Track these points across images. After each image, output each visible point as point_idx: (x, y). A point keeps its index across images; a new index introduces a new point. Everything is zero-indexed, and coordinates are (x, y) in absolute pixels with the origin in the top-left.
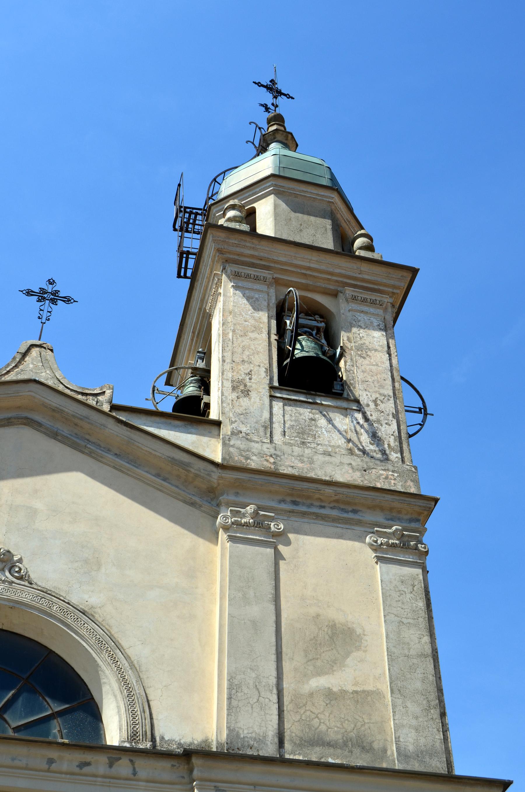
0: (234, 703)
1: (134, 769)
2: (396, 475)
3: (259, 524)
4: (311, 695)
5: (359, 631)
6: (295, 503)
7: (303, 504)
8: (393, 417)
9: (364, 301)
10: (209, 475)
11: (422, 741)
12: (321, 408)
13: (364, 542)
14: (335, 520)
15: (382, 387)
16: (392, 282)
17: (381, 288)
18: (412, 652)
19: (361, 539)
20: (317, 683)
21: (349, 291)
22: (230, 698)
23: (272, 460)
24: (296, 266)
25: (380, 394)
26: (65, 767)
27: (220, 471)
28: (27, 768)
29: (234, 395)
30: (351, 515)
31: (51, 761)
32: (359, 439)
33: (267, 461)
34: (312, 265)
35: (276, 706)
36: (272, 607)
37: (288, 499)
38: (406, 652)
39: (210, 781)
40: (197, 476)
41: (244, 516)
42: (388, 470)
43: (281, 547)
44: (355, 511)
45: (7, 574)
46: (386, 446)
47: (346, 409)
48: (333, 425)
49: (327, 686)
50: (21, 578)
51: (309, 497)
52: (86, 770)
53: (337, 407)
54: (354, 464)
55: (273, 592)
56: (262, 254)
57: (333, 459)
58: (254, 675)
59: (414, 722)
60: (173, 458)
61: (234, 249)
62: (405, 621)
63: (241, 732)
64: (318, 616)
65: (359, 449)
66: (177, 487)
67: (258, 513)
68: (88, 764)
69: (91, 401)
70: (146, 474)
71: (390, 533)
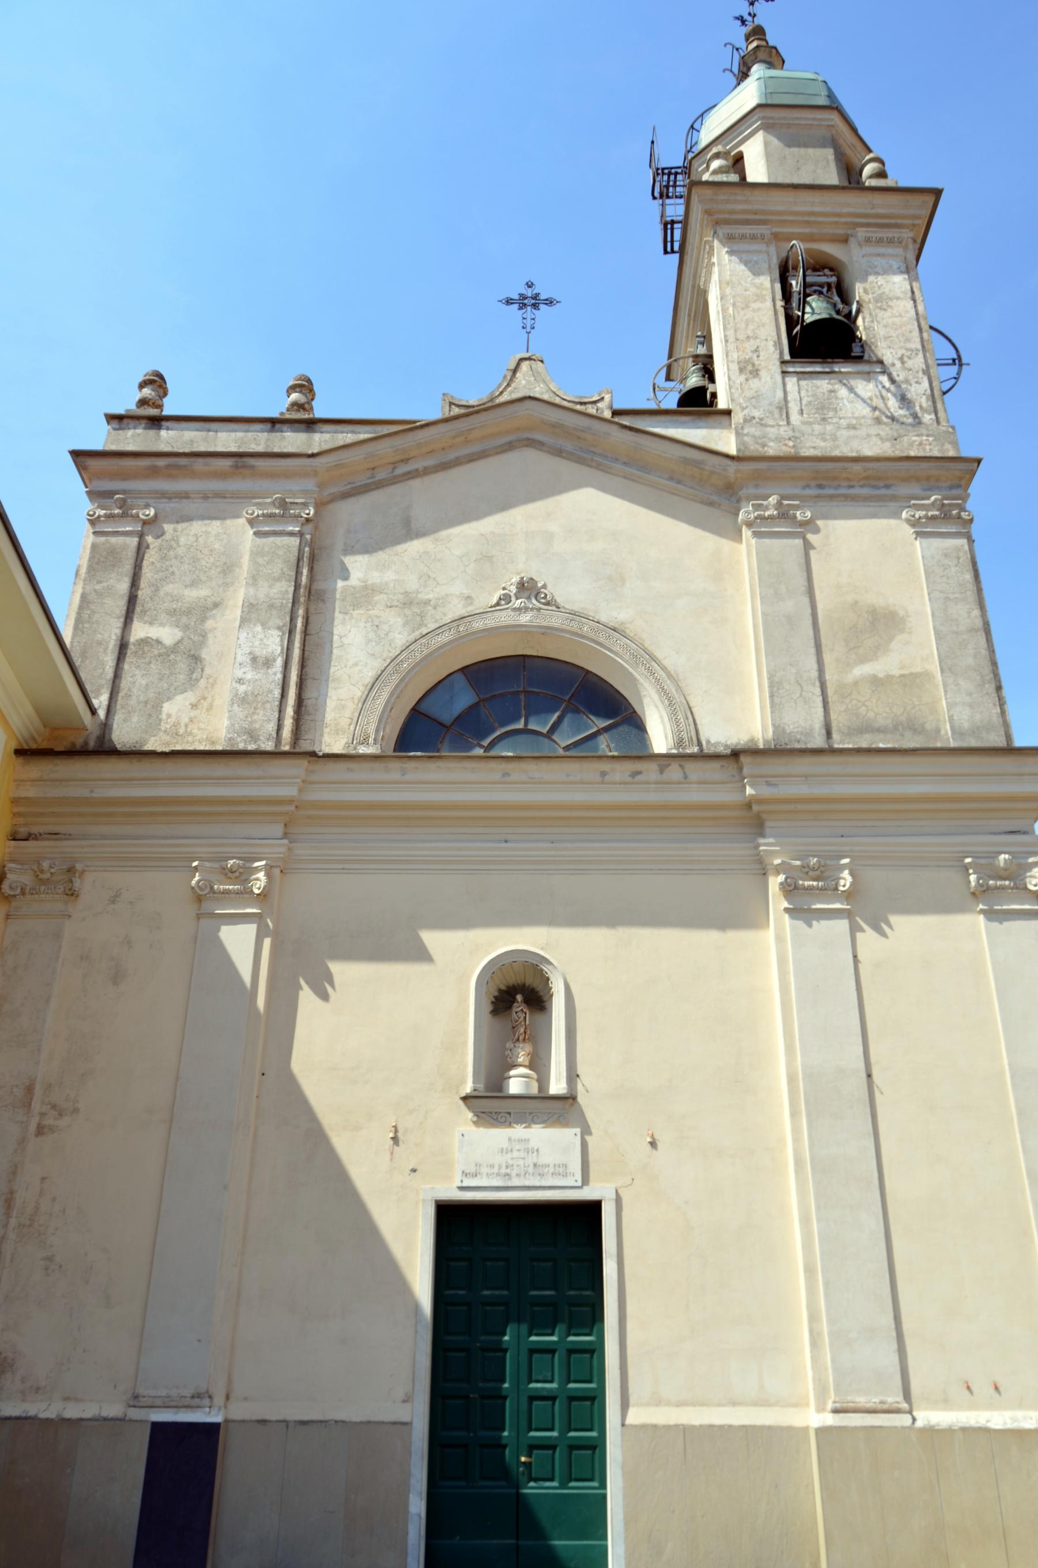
0: (777, 700)
1: (685, 773)
2: (931, 439)
3: (784, 515)
4: (856, 683)
5: (901, 613)
6: (820, 487)
7: (830, 487)
8: (924, 373)
9: (880, 241)
10: (725, 470)
11: (978, 717)
12: (840, 376)
13: (900, 518)
14: (866, 499)
15: (908, 340)
16: (911, 212)
17: (899, 221)
18: (962, 628)
19: (897, 515)
20: (860, 671)
21: (861, 233)
22: (772, 696)
23: (791, 444)
24: (797, 214)
25: (907, 350)
26: (618, 777)
27: (736, 463)
28: (582, 783)
29: (743, 378)
30: (883, 491)
31: (604, 774)
32: (886, 405)
33: (786, 445)
34: (817, 209)
35: (821, 698)
36: (806, 600)
37: (813, 483)
38: (955, 628)
39: (761, 776)
40: (712, 473)
41: (767, 508)
42: (922, 435)
43: (810, 537)
44: (887, 487)
45: (534, 601)
46: (917, 408)
47: (869, 373)
48: (856, 394)
49: (872, 672)
50: (548, 604)
51: (835, 478)
52: (638, 778)
53: (858, 373)
54: (882, 433)
55: (806, 584)
56: (756, 207)
57: (858, 433)
58: (794, 671)
59: (968, 699)
60: (685, 459)
61: (722, 207)
62: (951, 596)
63: (787, 727)
64: (856, 603)
65: (887, 417)
66: (692, 488)
67: (781, 504)
68: (639, 773)
69: (591, 410)
70: (657, 479)
71: (928, 505)
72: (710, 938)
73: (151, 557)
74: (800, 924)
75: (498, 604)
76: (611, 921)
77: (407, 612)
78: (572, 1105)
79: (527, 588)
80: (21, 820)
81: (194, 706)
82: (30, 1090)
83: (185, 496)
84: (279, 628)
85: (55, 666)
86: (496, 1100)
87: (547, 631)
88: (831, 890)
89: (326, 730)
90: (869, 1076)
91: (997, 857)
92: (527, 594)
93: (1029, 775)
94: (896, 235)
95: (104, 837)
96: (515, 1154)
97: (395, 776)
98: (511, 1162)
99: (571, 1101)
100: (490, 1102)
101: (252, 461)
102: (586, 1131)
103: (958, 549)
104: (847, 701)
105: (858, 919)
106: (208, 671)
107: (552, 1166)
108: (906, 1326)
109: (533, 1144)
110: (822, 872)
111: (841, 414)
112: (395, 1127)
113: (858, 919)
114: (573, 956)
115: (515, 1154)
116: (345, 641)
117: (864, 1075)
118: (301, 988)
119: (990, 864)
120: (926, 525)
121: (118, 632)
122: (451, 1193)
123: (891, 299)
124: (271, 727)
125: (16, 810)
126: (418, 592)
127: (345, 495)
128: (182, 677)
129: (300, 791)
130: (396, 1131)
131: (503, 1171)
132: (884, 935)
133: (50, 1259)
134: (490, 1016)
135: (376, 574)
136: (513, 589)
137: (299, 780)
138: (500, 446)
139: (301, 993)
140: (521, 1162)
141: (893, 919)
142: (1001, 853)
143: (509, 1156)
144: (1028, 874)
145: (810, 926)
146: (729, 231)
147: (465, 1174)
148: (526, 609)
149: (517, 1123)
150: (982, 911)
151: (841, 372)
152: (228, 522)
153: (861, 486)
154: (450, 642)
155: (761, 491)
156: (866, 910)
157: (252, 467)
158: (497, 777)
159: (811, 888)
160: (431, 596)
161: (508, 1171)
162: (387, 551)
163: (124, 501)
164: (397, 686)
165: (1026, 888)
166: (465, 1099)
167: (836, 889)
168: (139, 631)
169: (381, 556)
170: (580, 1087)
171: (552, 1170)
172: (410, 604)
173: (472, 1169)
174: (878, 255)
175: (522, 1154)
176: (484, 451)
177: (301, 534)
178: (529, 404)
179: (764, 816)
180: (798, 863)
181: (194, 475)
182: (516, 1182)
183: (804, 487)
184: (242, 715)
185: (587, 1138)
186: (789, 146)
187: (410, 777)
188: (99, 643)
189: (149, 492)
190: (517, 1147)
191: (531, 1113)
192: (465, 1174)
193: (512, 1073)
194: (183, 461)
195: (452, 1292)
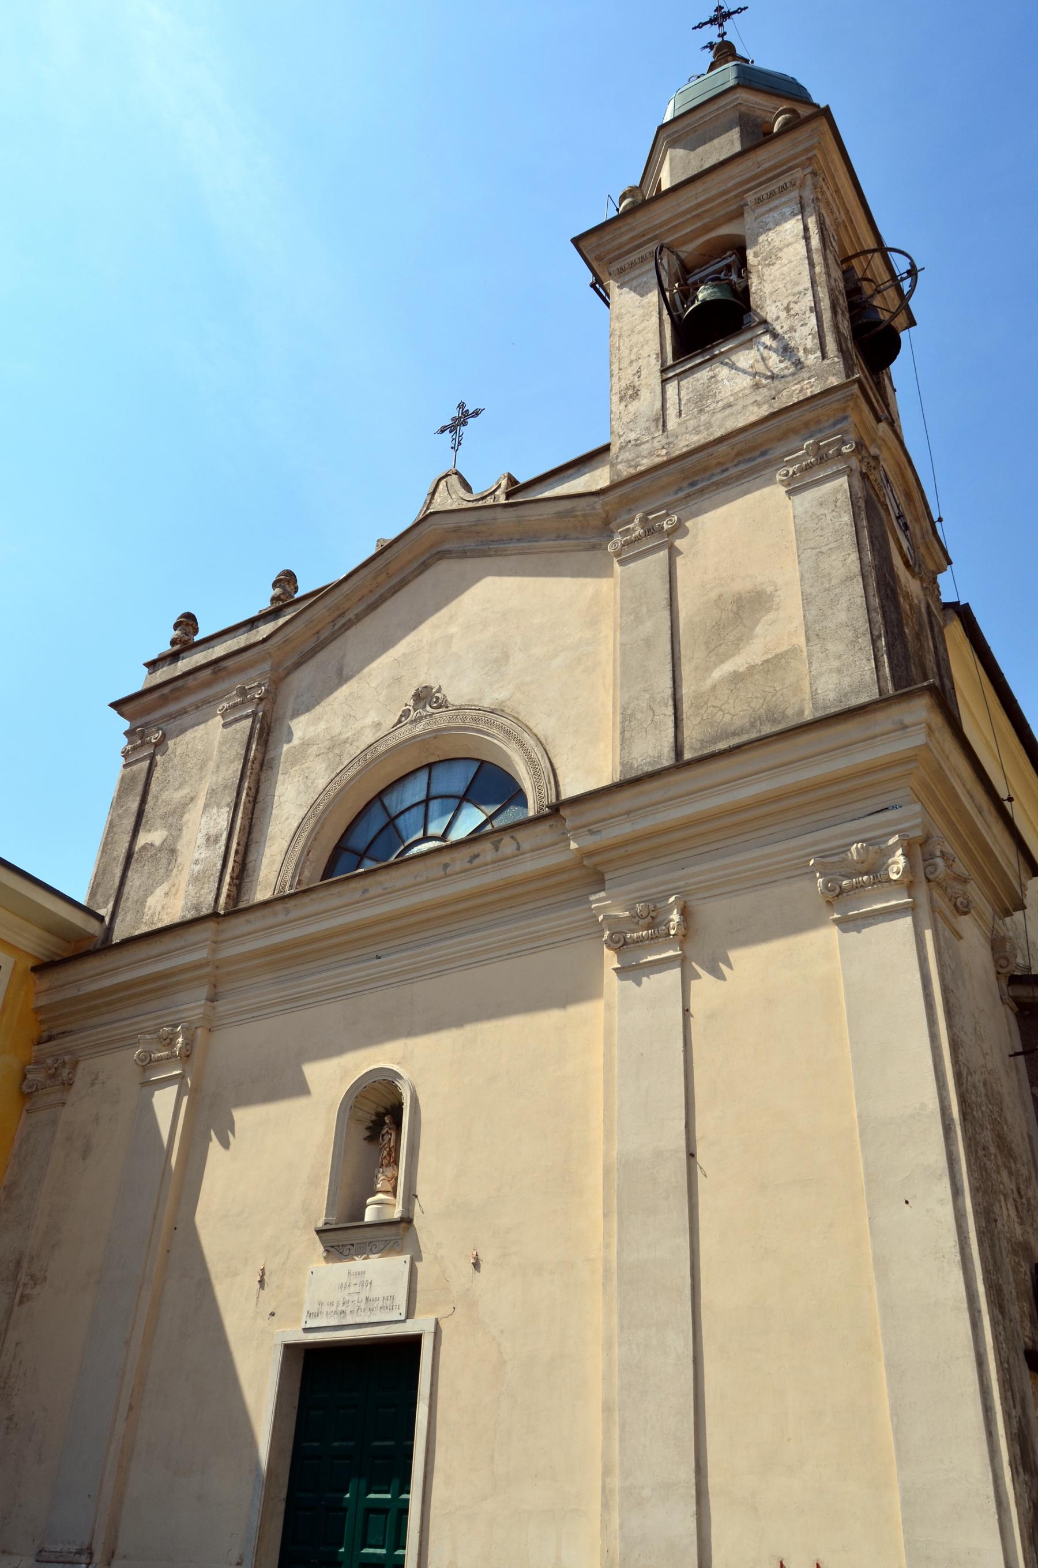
0: (627, 734)
1: (518, 844)
2: (813, 380)
3: (650, 531)
4: (714, 688)
5: (769, 589)
6: (692, 484)
7: (703, 480)
8: (811, 311)
9: (771, 195)
10: (593, 508)
11: (847, 680)
12: (721, 358)
13: (775, 483)
14: (739, 477)
15: (797, 284)
16: (801, 147)
17: (791, 164)
18: (834, 581)
19: (771, 481)
20: (717, 674)
21: (750, 198)
22: (623, 732)
23: (664, 452)
24: (683, 213)
25: (794, 295)
26: (458, 867)
27: (602, 497)
28: (428, 881)
29: (622, 406)
30: (760, 460)
31: (446, 866)
32: (766, 365)
33: (658, 456)
34: (700, 200)
35: (673, 718)
36: (666, 614)
37: (685, 484)
38: (827, 585)
39: (584, 826)
40: (584, 516)
41: (634, 530)
42: (803, 380)
43: (679, 543)
44: (763, 454)
45: (428, 708)
46: (801, 353)
47: (751, 340)
48: (737, 369)
49: (731, 670)
50: (440, 707)
51: (705, 469)
52: (476, 862)
53: (740, 345)
54: (759, 398)
55: (668, 596)
56: (642, 229)
57: (735, 408)
58: (647, 696)
59: (836, 664)
60: (558, 513)
61: (608, 247)
62: (824, 549)
63: (635, 762)
64: (721, 596)
65: (767, 378)
66: (577, 538)
67: (647, 519)
68: (477, 856)
69: (490, 501)
70: (547, 543)
71: (803, 455)
72: (551, 1018)
73: (157, 773)
74: (630, 984)
75: (400, 721)
76: (459, 1022)
77: (331, 755)
78: (408, 1229)
79: (424, 696)
80: (44, 1027)
81: (166, 894)
82: (18, 1263)
83: (184, 712)
84: (228, 805)
85: (13, 891)
86: (339, 1232)
87: (437, 734)
88: (659, 936)
89: (259, 888)
90: (691, 1155)
91: (849, 850)
92: (422, 703)
93: (882, 735)
94: (787, 180)
95: (95, 1027)
96: (353, 1289)
97: (281, 918)
98: (347, 1298)
99: (403, 1225)
100: (345, 1234)
101: (225, 664)
102: (416, 1257)
103: (836, 491)
104: (702, 711)
105: (694, 964)
106: (179, 860)
107: (381, 1299)
108: (713, 1481)
109: (367, 1277)
110: (653, 918)
111: (719, 397)
112: (263, 1270)
113: (694, 964)
114: (422, 1063)
115: (353, 1289)
116: (282, 799)
117: (683, 1155)
118: (211, 1139)
119: (844, 860)
120: (801, 478)
121: (127, 845)
122: (298, 1336)
123: (781, 250)
124: (211, 897)
125: (40, 1018)
126: (340, 734)
127: (298, 665)
128: (162, 871)
129: (214, 951)
130: (263, 1274)
131: (340, 1308)
132: (721, 976)
133: (10, 1418)
134: (365, 1143)
135: (312, 728)
136: (412, 702)
137: (209, 942)
138: (415, 570)
139: (211, 1144)
140: (356, 1297)
141: (733, 955)
142: (853, 844)
143: (347, 1291)
144: (890, 861)
145: (639, 983)
146: (618, 266)
147: (309, 1314)
148: (421, 718)
149: (357, 1255)
150: (836, 922)
151: (722, 353)
152: (209, 723)
153: (736, 466)
154: (358, 773)
155: (626, 517)
156: (698, 949)
157: (225, 668)
158: (357, 896)
159: (641, 940)
160: (349, 734)
161: (344, 1308)
162: (323, 704)
163: (143, 732)
164: (313, 829)
165: (889, 880)
166: (319, 1232)
167: (669, 935)
168: (143, 839)
169: (318, 709)
170: (417, 1209)
171: (380, 1304)
172: (335, 744)
173: (314, 1309)
174: (771, 210)
175: (357, 1289)
176: (403, 580)
177: (254, 714)
178: (431, 519)
179: (600, 868)
180: (627, 914)
181: (190, 691)
182: (349, 1320)
183: (676, 493)
184: (193, 893)
185: (418, 1264)
186: (693, 149)
187: (293, 915)
188: (115, 859)
189: (162, 718)
190: (354, 1282)
191: (370, 1243)
192: (309, 1314)
193: (369, 1201)
194: (179, 683)
195: (308, 1444)
